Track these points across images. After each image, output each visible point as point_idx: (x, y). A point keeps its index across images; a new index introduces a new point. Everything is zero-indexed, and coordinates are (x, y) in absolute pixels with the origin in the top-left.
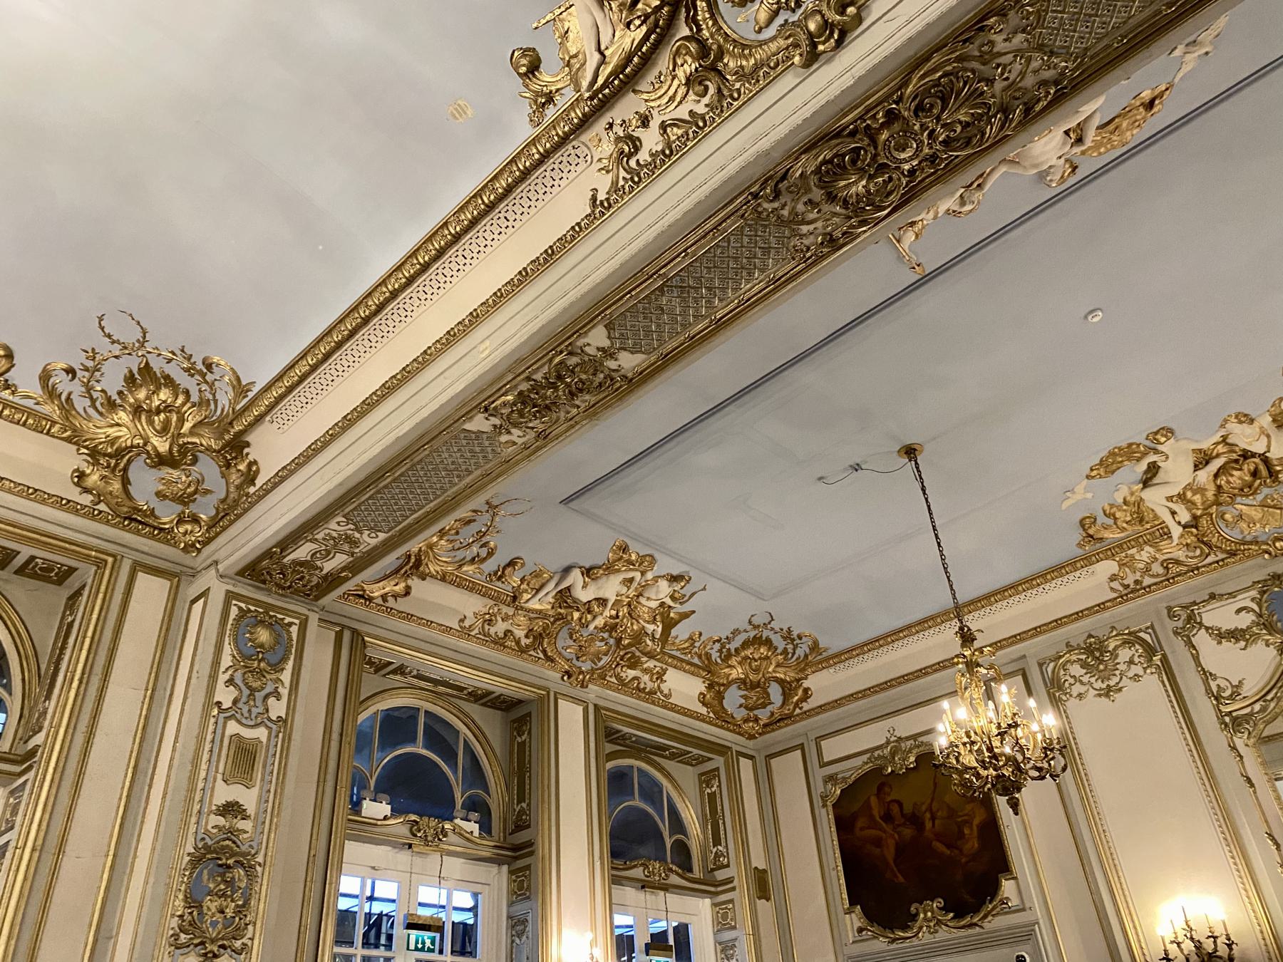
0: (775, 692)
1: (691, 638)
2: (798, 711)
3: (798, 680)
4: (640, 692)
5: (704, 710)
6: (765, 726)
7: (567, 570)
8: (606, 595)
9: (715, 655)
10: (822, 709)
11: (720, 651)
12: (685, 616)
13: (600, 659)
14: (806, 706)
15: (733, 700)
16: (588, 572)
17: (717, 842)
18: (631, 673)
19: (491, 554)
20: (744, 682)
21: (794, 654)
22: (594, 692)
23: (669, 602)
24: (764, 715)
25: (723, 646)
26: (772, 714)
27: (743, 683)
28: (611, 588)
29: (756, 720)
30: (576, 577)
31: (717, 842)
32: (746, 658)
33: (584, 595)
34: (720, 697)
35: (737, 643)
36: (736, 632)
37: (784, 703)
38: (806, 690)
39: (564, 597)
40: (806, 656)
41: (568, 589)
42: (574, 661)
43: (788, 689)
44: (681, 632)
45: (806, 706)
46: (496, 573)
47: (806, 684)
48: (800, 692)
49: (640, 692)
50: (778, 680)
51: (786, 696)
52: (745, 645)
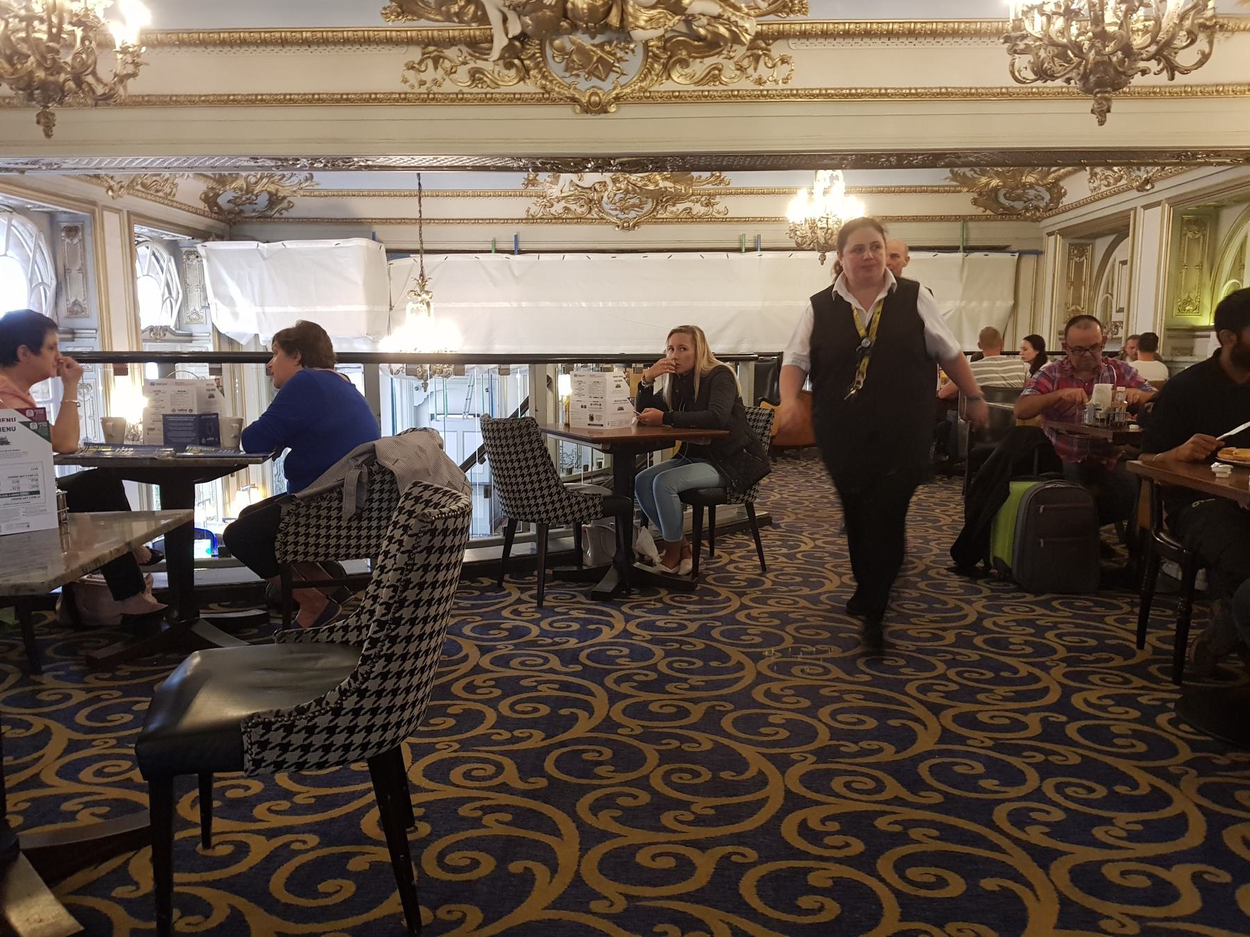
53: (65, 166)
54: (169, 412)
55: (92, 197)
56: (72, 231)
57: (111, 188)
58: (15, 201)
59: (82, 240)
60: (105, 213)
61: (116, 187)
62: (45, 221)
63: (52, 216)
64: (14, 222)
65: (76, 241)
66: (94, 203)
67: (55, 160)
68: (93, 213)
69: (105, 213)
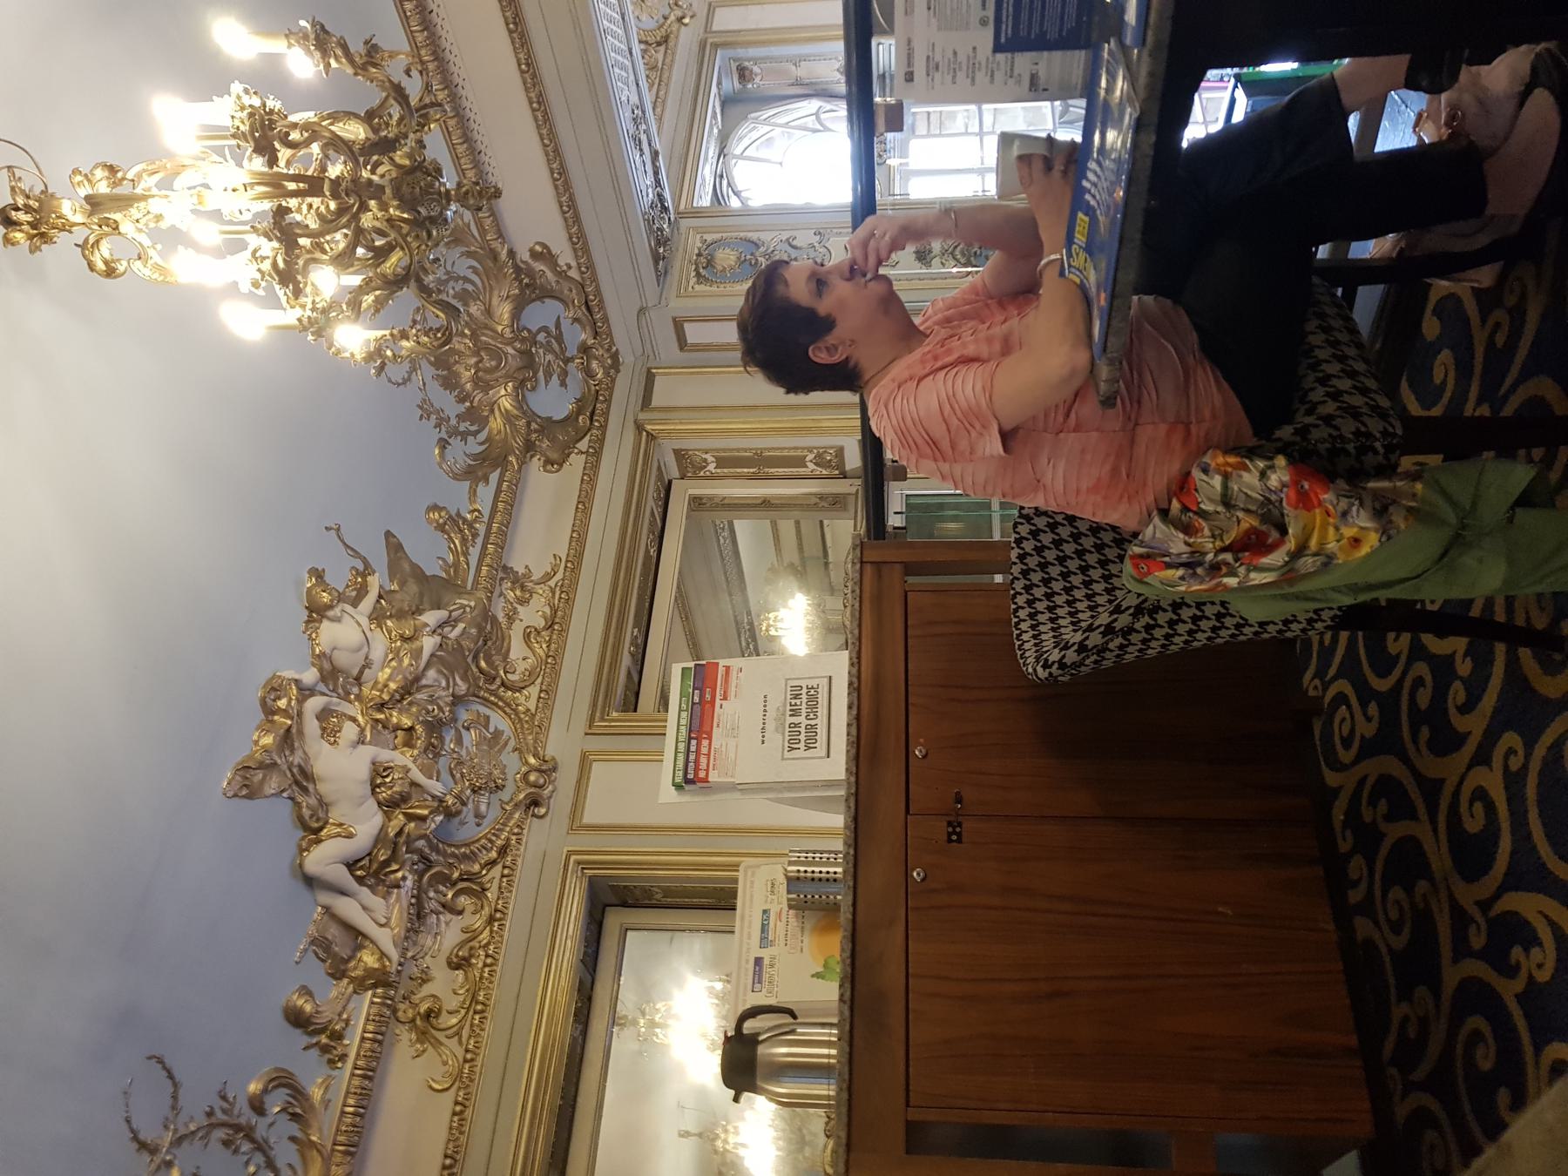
0: (541, 315)
1: (441, 528)
2: (573, 274)
3: (518, 270)
4: (556, 623)
5: (576, 462)
6: (596, 334)
7: (311, 882)
8: (364, 772)
9: (474, 446)
10: (579, 241)
11: (464, 436)
12: (394, 547)
13: (497, 734)
14: (566, 257)
15: (553, 401)
16: (312, 829)
17: (801, 462)
18: (517, 649)
19: (283, 1080)
20: (521, 385)
21: (466, 280)
22: (563, 740)
23: (368, 603)
24: (577, 336)
25: (454, 432)
26: (576, 320)
27: (522, 386)
28: (342, 764)
29: (585, 349)
30: (325, 858)
31: (801, 462)
32: (476, 381)
33: (365, 825)
34: (548, 426)
35: (449, 405)
36: (426, 409)
37: (561, 300)
38: (534, 255)
39: (370, 870)
40: (469, 254)
41: (351, 866)
42: (505, 795)
43: (530, 291)
44: (429, 552)
45: (566, 257)
46: (325, 1049)
47: (524, 255)
48: (539, 266)
49: (556, 623)
50: (516, 315)
51: (546, 294)
52: (450, 382)
53: (635, 99)
54: (988, 34)
55: (695, 48)
56: (743, 74)
57: (680, 20)
58: (711, 149)
59: (756, 61)
60: (715, 28)
61: (679, 13)
62: (734, 111)
63: (726, 102)
64: (738, 151)
65: (756, 69)
66: (703, 45)
67: (628, 114)
68: (716, 46)
69: (715, 28)
